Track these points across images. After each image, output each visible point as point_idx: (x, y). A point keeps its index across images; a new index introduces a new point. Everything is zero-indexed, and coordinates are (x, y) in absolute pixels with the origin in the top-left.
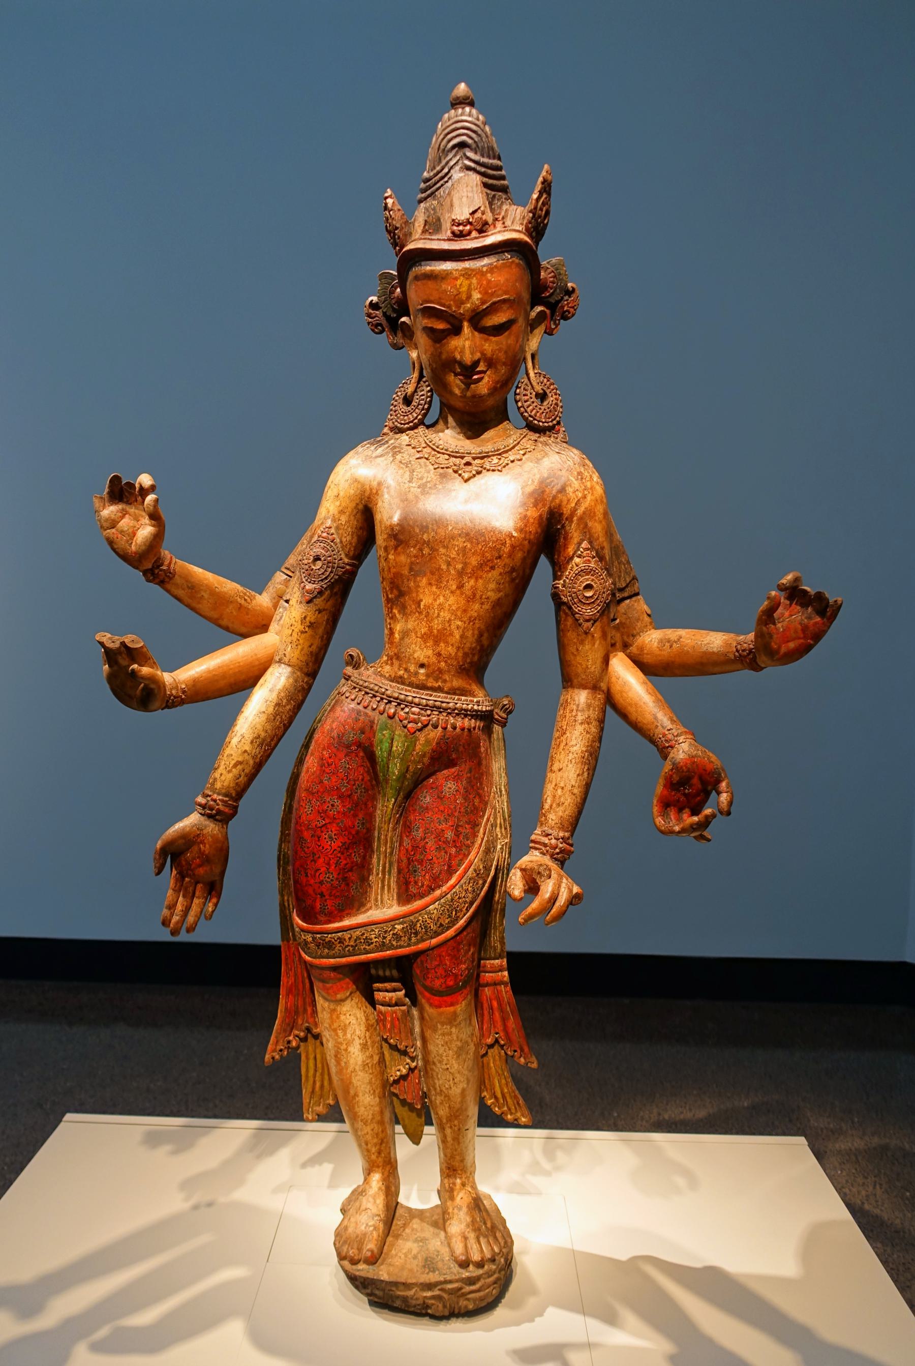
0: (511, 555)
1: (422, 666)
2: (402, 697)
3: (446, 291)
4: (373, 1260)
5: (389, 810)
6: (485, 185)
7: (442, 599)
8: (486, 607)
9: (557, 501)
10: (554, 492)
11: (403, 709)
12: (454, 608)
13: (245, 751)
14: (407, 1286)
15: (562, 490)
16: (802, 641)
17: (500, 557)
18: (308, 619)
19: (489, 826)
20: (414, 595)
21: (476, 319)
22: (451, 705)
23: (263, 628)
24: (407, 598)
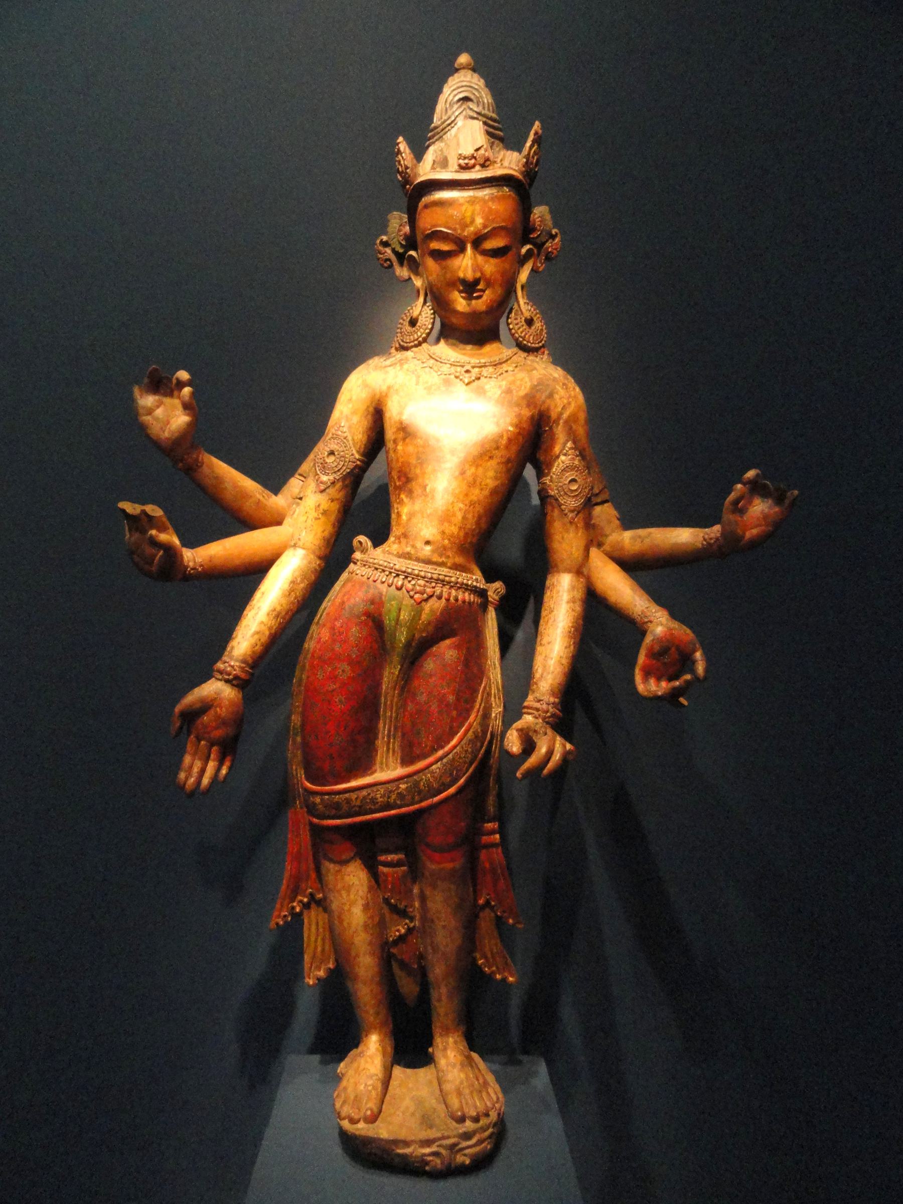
0: (507, 447)
1: (428, 543)
2: (410, 570)
3: (452, 216)
4: (373, 1119)
8: (486, 492)
9: (546, 406)
10: (543, 397)
11: (410, 582)
12: (457, 491)
14: (406, 1144)
16: (763, 528)
17: (497, 448)
18: (322, 507)
19: (485, 695)
20: (420, 480)
21: (478, 241)
22: (453, 579)
23: (279, 523)
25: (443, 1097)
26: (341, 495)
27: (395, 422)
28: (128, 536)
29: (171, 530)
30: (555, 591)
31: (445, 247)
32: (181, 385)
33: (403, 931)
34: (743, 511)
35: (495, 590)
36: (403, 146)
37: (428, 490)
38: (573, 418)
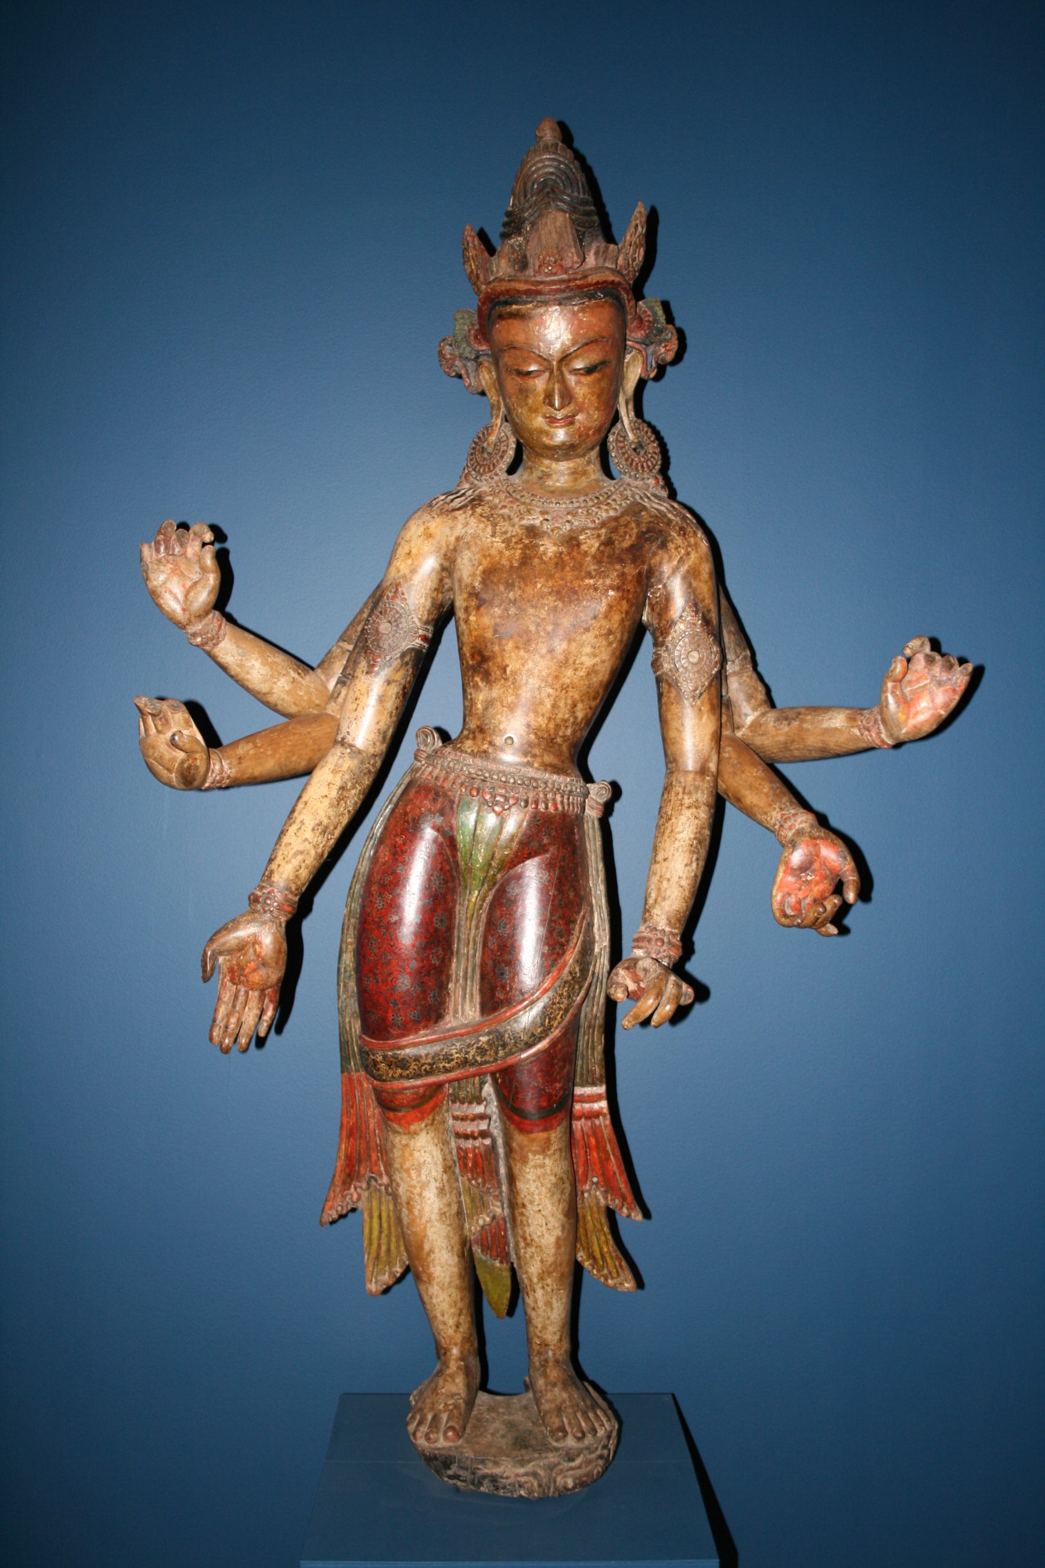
5: (472, 904)
7: (530, 664)
12: (544, 674)
13: (306, 840)
20: (499, 660)
24: (490, 664)
30: (673, 794)
33: (488, 1219)
37: (508, 672)
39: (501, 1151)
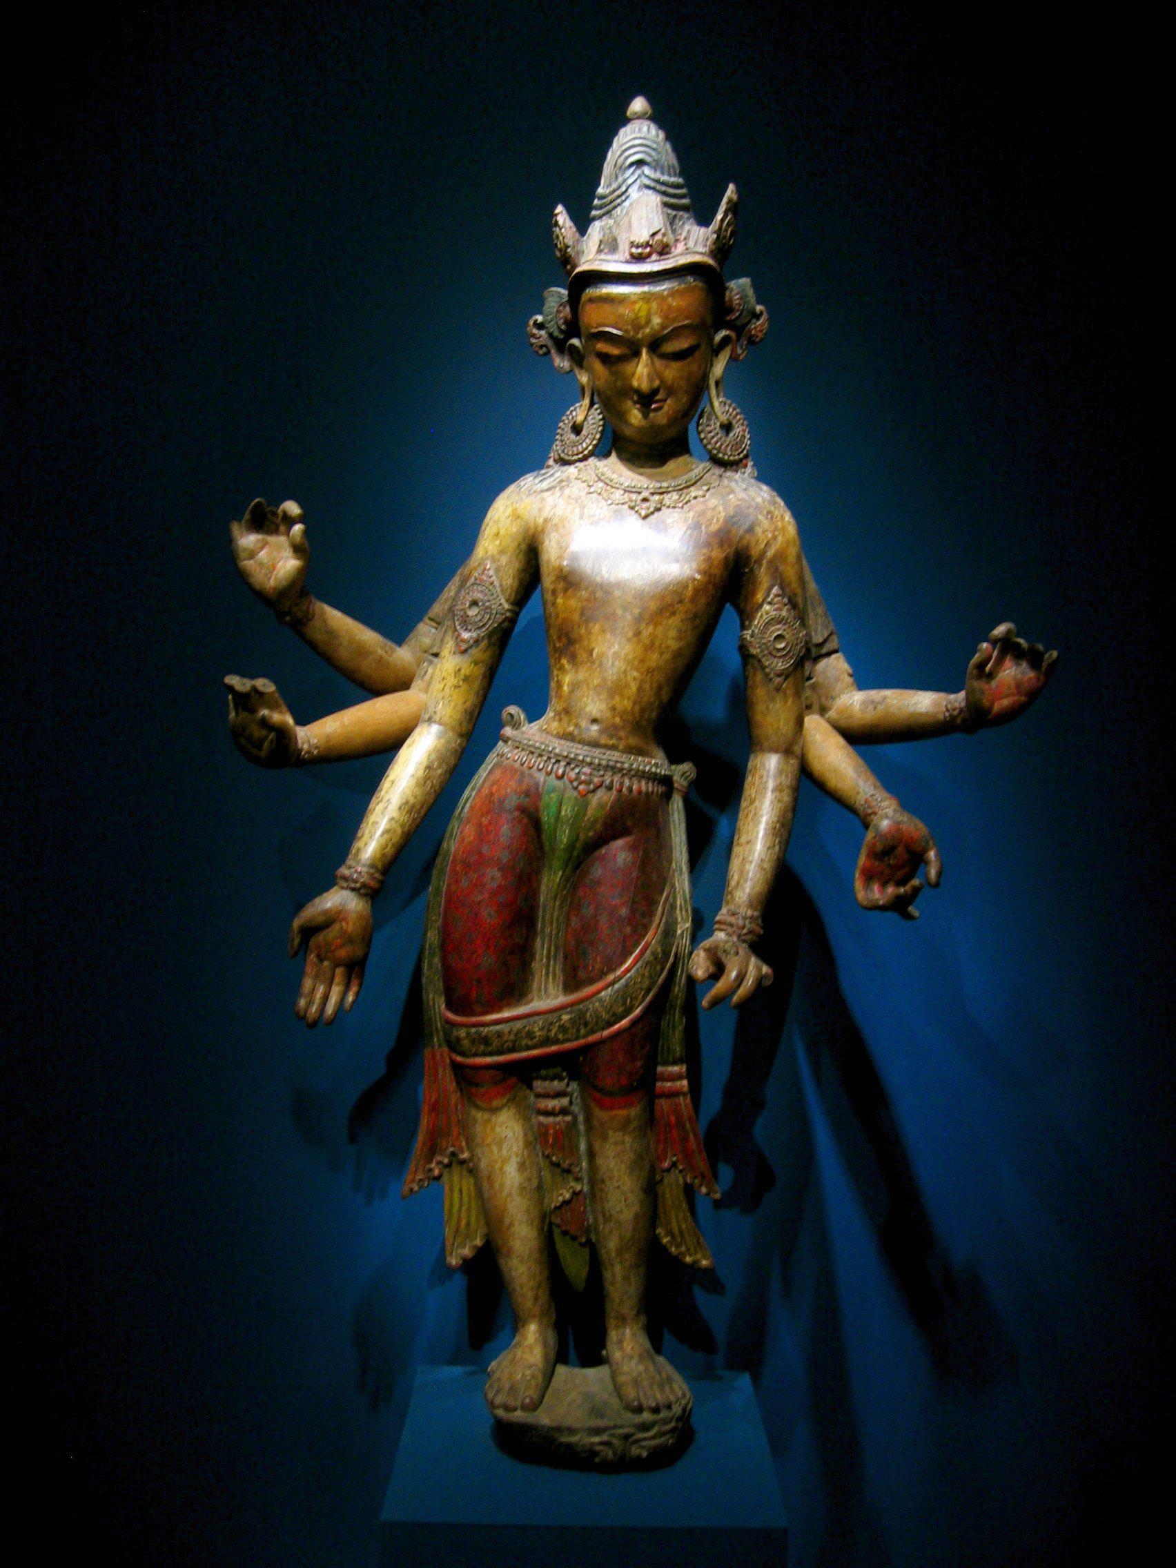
0: (693, 600)
1: (594, 721)
3: (621, 316)
4: (534, 1407)
6: (666, 205)
7: (616, 647)
8: (667, 656)
9: (745, 542)
10: (741, 532)
12: (630, 657)
14: (572, 1431)
15: (750, 530)
16: (1016, 698)
17: (681, 602)
18: (463, 672)
20: (586, 643)
21: (655, 345)
22: (626, 766)
23: (405, 685)
25: (617, 1388)
26: (486, 657)
27: (554, 569)
28: (233, 715)
29: (284, 708)
31: (615, 351)
32: (289, 521)
34: (990, 676)
35: (683, 773)
36: (562, 215)
38: (781, 556)
39: (582, 1128)
